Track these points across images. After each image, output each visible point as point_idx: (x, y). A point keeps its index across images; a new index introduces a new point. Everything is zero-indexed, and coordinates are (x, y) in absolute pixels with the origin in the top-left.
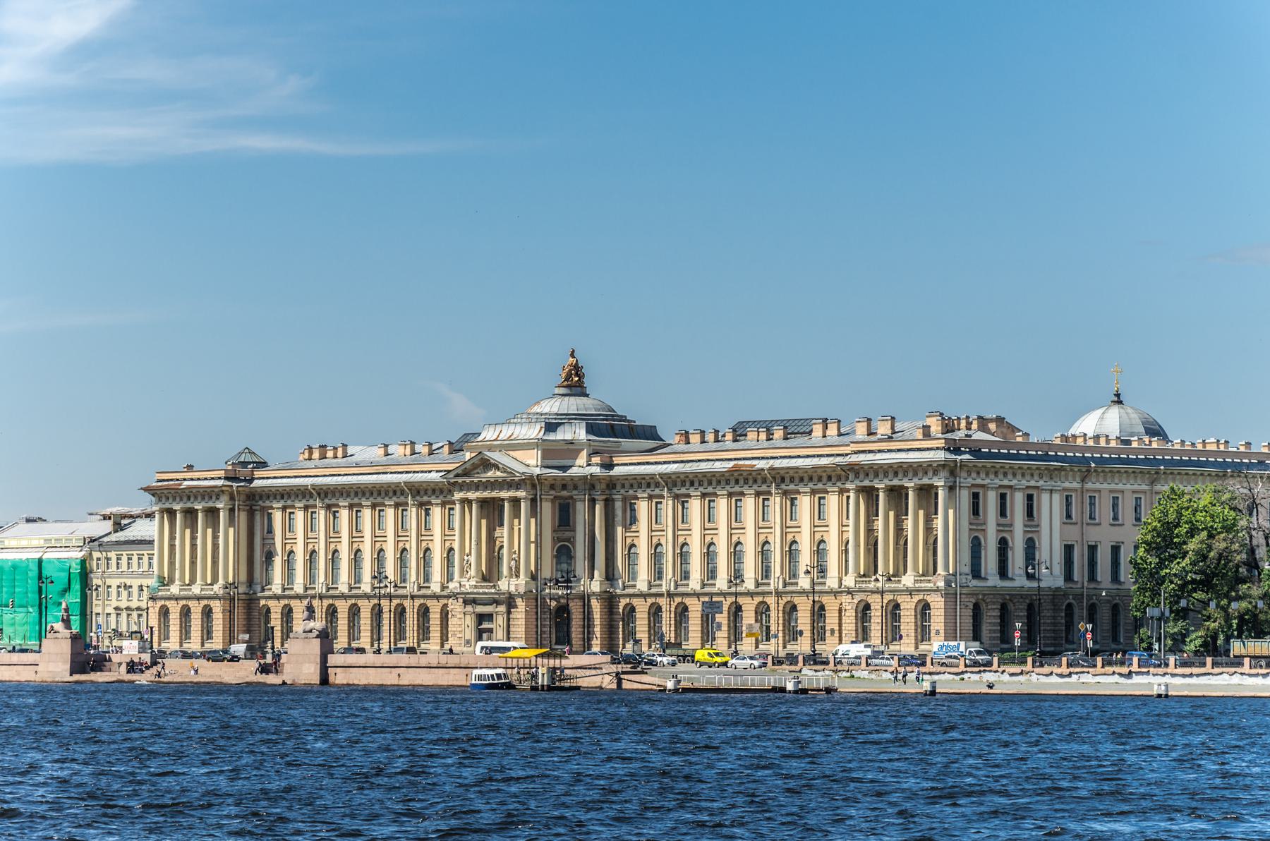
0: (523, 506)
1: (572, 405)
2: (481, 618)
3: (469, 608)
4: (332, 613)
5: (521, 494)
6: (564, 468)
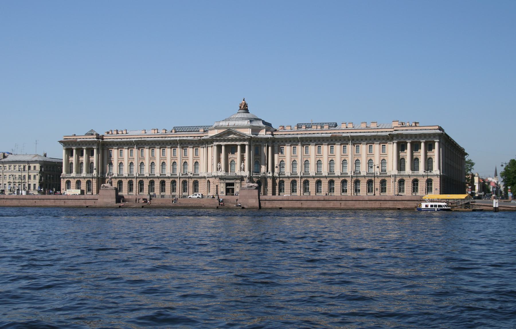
0: (247, 147)
1: (245, 115)
2: (227, 184)
3: (222, 181)
4: (120, 183)
5: (246, 143)
6: (257, 135)
